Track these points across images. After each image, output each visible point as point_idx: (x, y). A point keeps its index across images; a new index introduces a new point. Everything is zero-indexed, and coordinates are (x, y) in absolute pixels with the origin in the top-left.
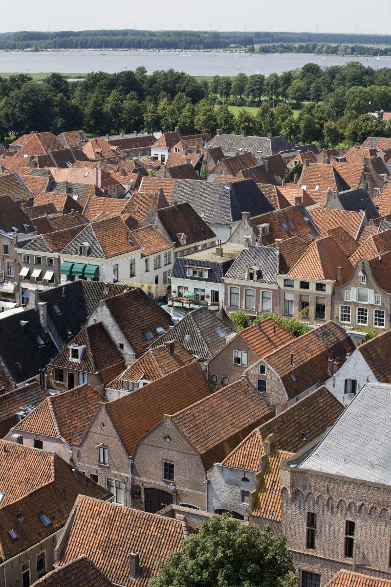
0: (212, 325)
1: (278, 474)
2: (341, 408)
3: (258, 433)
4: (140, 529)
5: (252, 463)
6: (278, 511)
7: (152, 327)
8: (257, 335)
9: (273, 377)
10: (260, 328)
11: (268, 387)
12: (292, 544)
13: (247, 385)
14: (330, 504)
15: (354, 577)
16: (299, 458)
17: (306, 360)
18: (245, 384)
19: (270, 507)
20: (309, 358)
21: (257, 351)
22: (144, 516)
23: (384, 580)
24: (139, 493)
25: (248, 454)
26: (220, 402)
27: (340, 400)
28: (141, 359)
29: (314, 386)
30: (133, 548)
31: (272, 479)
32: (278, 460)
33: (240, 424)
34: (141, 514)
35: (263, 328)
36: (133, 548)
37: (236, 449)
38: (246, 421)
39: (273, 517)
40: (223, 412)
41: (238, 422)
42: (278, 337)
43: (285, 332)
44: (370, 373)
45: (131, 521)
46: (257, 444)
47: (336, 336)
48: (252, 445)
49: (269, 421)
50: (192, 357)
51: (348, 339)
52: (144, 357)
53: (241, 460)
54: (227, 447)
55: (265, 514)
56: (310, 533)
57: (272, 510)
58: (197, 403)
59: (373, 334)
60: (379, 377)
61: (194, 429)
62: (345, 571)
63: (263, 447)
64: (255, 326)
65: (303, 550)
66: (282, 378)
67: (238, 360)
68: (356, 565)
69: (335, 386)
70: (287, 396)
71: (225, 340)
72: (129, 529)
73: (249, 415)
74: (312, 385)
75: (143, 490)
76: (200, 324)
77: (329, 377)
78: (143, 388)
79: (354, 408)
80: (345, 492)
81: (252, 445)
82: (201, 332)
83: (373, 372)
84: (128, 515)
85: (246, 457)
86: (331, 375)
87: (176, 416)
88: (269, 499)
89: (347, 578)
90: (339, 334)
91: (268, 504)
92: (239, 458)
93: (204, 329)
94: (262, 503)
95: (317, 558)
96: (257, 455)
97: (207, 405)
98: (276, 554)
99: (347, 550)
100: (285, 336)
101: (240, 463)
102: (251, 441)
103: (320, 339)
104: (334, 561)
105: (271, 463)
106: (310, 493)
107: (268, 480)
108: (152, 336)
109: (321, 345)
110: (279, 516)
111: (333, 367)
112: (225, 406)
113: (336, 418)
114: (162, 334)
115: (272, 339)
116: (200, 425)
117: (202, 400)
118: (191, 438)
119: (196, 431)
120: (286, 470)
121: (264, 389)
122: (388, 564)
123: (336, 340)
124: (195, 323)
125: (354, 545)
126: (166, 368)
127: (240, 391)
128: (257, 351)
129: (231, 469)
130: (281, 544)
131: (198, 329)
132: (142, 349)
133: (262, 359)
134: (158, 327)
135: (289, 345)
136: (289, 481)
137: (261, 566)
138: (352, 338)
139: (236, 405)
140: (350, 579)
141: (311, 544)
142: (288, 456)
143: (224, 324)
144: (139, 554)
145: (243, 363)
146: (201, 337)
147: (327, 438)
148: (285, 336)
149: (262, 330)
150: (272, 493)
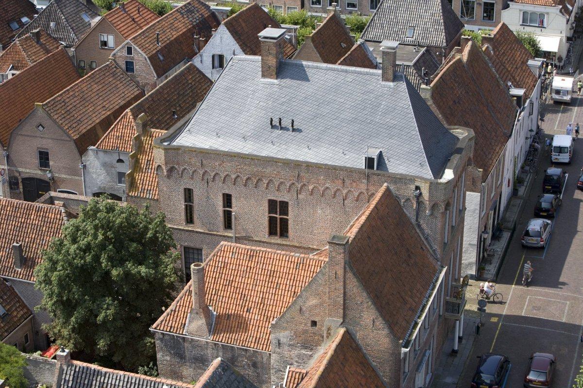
0: (76, 11)
1: (152, 152)
2: (210, 83)
3: (130, 114)
4: (20, 219)
5: (125, 144)
6: (155, 189)
7: (17, 17)
8: (122, 17)
9: (141, 57)
10: (124, 9)
11: (136, 67)
12: (171, 221)
13: (115, 67)
14: (205, 178)
15: (235, 248)
16: (172, 135)
17: (172, 39)
18: (113, 67)
19: (147, 186)
20: (175, 36)
21: (123, 33)
22: (24, 206)
23: (265, 249)
24: (17, 184)
25: (121, 136)
26: (89, 86)
27: (209, 76)
28: (8, 50)
29: (182, 63)
30: (16, 239)
31: (146, 158)
32: (151, 139)
33: (111, 107)
34: (20, 204)
35: (127, 10)
36: (16, 239)
37: (109, 131)
38: (116, 103)
39: (151, 195)
40: (93, 96)
41: (109, 105)
42: (143, 18)
43: (149, 12)
44: (237, 47)
45: (11, 212)
46: (129, 125)
47: (200, 13)
48: (124, 127)
49: (139, 101)
50: (59, 44)
51: (213, 15)
52: (10, 48)
53: (114, 142)
54: (99, 131)
55: (142, 194)
56: (188, 208)
57: (149, 189)
58: (66, 89)
59: (237, 8)
60: (246, 50)
61: (65, 115)
62: (225, 243)
63: (135, 127)
64: (119, 8)
65: (183, 226)
66: (149, 58)
67: (105, 43)
68: (236, 237)
69: (203, 62)
70: (155, 75)
71: (90, 24)
72: (10, 221)
73: (119, 97)
74: (179, 63)
75: (20, 181)
76: (64, 11)
77: (196, 54)
78: (12, 79)
79: (222, 82)
80: (220, 165)
81: (124, 127)
82: (65, 18)
83: (240, 46)
84: (8, 206)
85: (119, 139)
86: (198, 51)
87: (46, 104)
88: (145, 178)
89: (229, 250)
90: (203, 10)
91: (144, 183)
92: (112, 140)
93: (68, 15)
94: (138, 182)
95: (197, 232)
96: (130, 136)
97: (77, 90)
98: (156, 232)
99: (226, 223)
100: (150, 16)
101: (114, 145)
102: (122, 122)
103: (185, 16)
104: (214, 235)
105: (144, 143)
106: (185, 169)
107: (142, 159)
108: (18, 27)
109: (186, 22)
110: (157, 194)
111: (199, 44)
112: (95, 90)
113: (205, 94)
114: (27, 24)
115: (136, 20)
116: (71, 111)
117: (71, 86)
118: (64, 124)
119: (68, 117)
120: (159, 148)
121: (132, 70)
122: (267, 233)
123: (200, 16)
124: (59, 10)
125: (233, 218)
126: (33, 57)
127: (108, 73)
128: (123, 33)
129: (105, 152)
130: (160, 222)
131: (62, 15)
132: (8, 40)
133: (128, 40)
134: (23, 17)
135: (154, 24)
136: (163, 158)
137: (143, 245)
138: (217, 13)
139: (105, 88)
140: (232, 250)
141: (190, 220)
142: (160, 134)
143: (89, 9)
144: (22, 244)
145: (110, 46)
146: (66, 23)
147: (197, 113)
148: (150, 16)
149: (126, 12)
150: (148, 173)
